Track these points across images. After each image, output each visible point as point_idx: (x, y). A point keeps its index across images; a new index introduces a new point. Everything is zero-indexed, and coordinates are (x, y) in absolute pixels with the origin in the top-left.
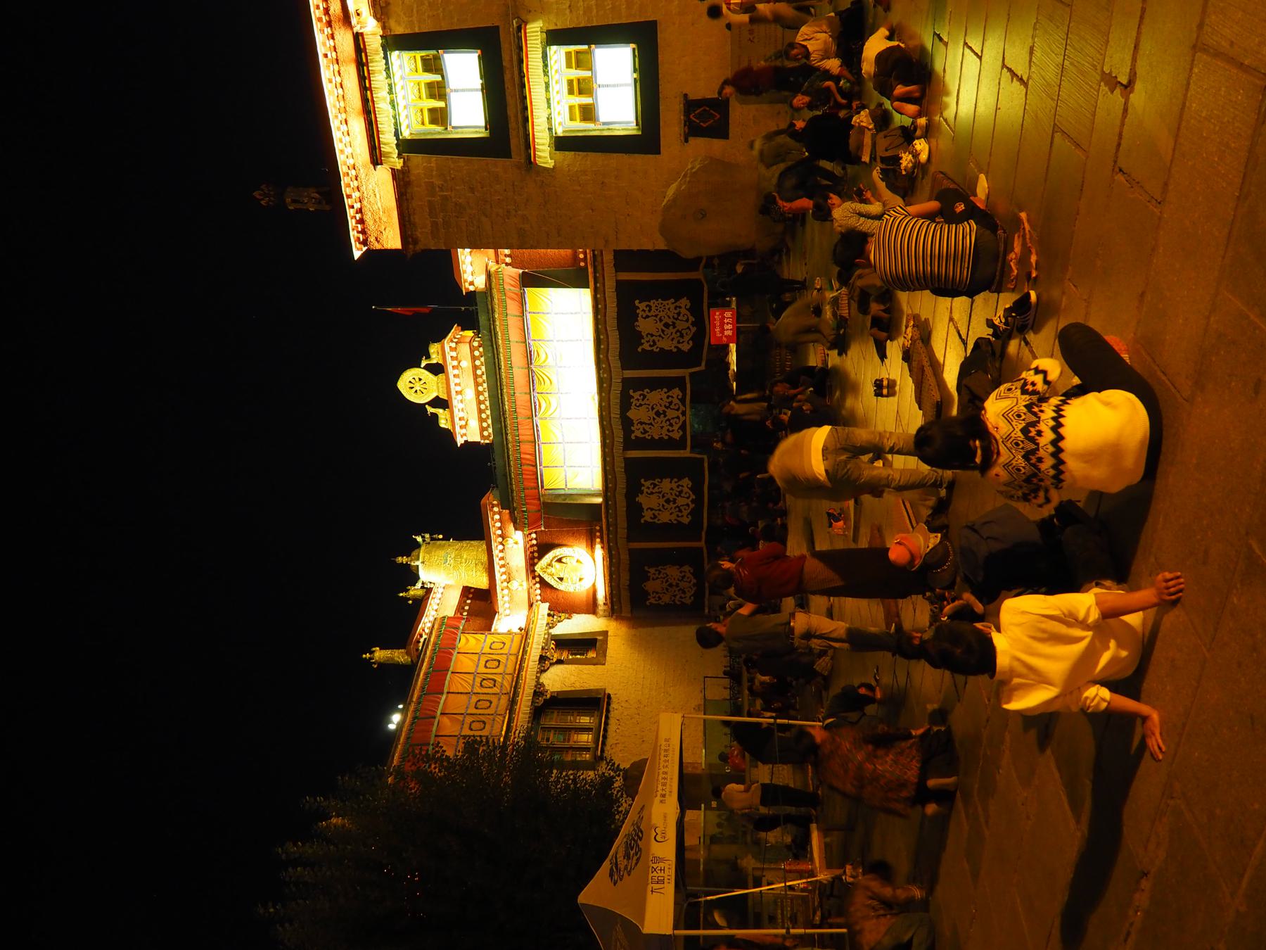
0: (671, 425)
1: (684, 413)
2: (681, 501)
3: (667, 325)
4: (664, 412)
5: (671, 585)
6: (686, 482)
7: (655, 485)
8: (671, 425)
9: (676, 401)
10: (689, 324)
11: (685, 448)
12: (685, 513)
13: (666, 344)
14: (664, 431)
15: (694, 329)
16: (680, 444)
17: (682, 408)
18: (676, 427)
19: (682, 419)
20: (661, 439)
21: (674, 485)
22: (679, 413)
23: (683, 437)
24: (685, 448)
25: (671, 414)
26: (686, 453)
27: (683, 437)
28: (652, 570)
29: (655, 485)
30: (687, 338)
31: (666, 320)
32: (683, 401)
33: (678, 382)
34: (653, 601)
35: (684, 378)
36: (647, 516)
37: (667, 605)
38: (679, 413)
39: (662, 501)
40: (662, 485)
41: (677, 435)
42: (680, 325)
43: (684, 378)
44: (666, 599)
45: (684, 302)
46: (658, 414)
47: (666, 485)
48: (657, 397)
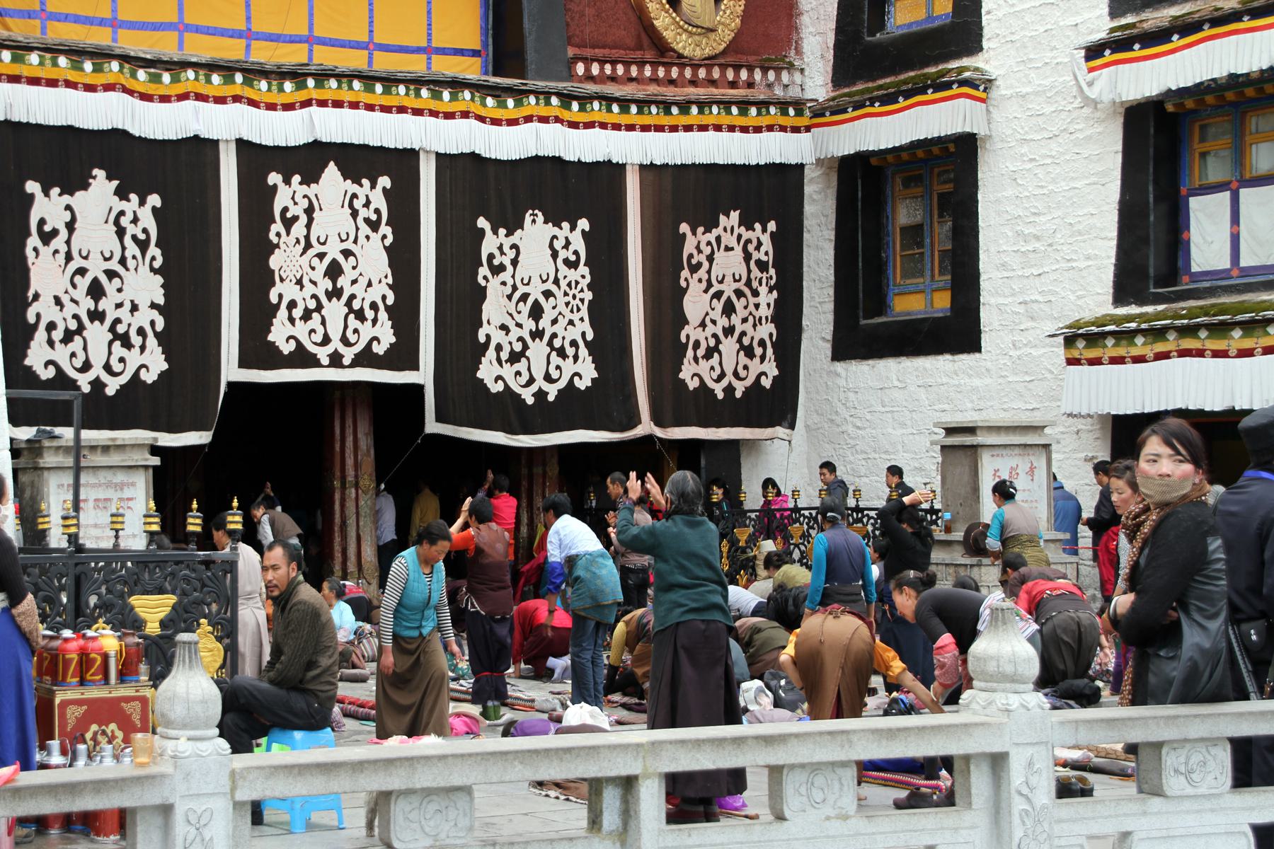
0: (307, 316)
1: (336, 360)
7: (143, 245)
8: (307, 316)
10: (540, 383)
11: (244, 363)
17: (348, 355)
19: (323, 354)
23: (273, 359)
24: (244, 363)
38: (336, 344)
41: (280, 334)
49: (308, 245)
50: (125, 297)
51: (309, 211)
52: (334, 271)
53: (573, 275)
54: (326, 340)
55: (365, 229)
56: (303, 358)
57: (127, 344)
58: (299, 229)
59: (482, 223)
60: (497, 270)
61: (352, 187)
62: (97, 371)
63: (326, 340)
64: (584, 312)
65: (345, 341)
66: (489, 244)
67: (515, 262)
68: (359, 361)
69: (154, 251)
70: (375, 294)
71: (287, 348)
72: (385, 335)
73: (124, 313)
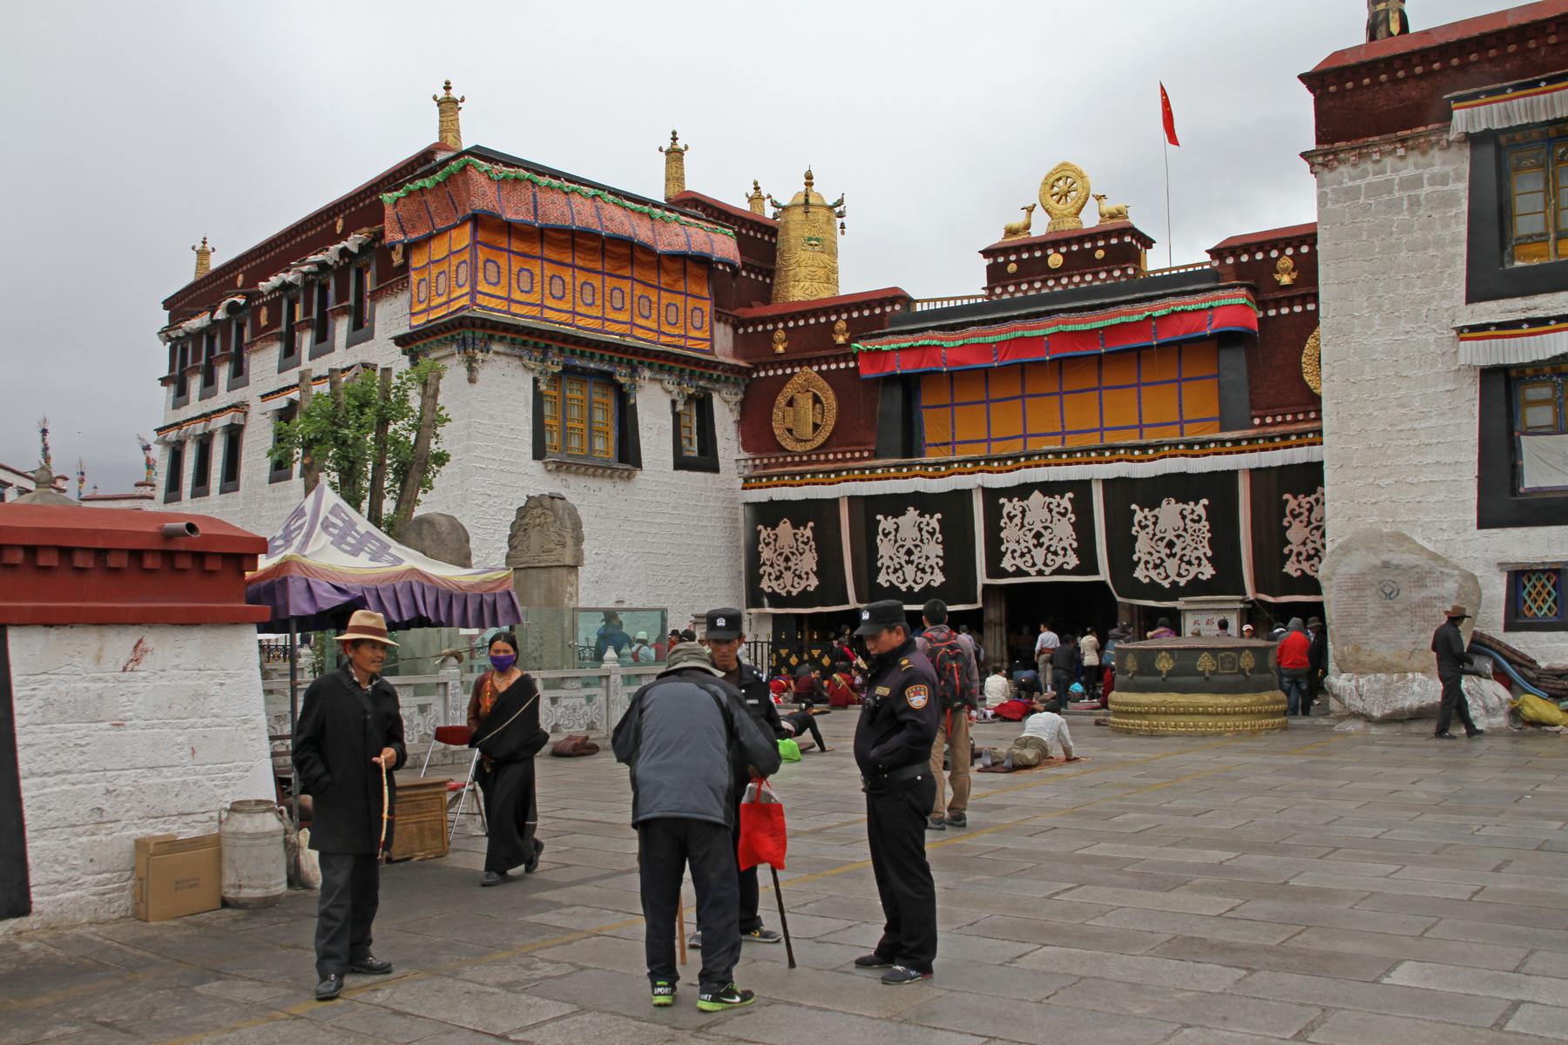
0: (1023, 555)
1: (1040, 573)
2: (910, 570)
3: (1171, 545)
4: (1041, 545)
5: (787, 559)
6: (938, 579)
7: (932, 534)
8: (1023, 555)
9: (1059, 560)
10: (1174, 577)
12: (893, 578)
13: (1142, 547)
14: (1012, 546)
15: (1166, 584)
16: (994, 569)
17: (1048, 571)
18: (1019, 562)
19: (1032, 571)
20: (1001, 542)
21: (933, 561)
22: (1040, 566)
23: (1004, 574)
25: (1039, 554)
26: (982, 578)
27: (1004, 574)
28: (808, 533)
29: (932, 534)
30: (1153, 574)
31: (1179, 544)
32: (1060, 571)
33: (1088, 563)
34: (764, 534)
35: (1097, 572)
36: (886, 523)
37: (759, 554)
38: (1040, 566)
39: (909, 544)
40: (933, 543)
41: (1007, 564)
42: (1172, 565)
43: (1097, 572)
44: (766, 554)
45: (1207, 572)
46: (1038, 535)
47: (934, 550)
48: (1064, 532)
49: (1023, 526)
50: (924, 553)
51: (1023, 512)
52: (1038, 535)
53: (1196, 526)
54: (1034, 565)
55: (1057, 516)
56: (1019, 572)
57: (923, 571)
58: (1017, 520)
59: (1134, 507)
60: (1144, 528)
61: (1048, 499)
62: (910, 582)
63: (1034, 565)
64: (1205, 543)
65: (1045, 564)
66: (1139, 516)
67: (1155, 524)
68: (1053, 573)
69: (938, 535)
70: (1065, 543)
71: (1011, 570)
72: (1073, 561)
73: (923, 561)
